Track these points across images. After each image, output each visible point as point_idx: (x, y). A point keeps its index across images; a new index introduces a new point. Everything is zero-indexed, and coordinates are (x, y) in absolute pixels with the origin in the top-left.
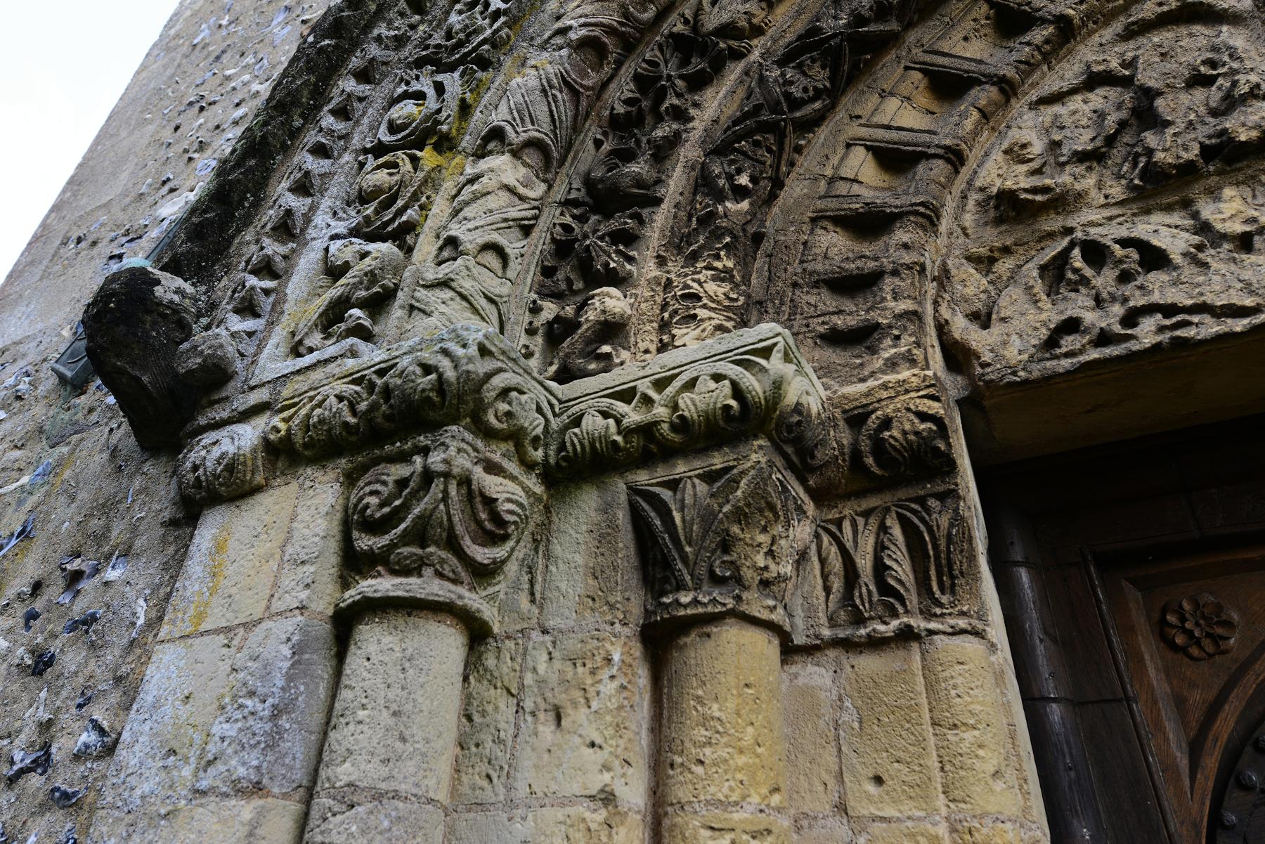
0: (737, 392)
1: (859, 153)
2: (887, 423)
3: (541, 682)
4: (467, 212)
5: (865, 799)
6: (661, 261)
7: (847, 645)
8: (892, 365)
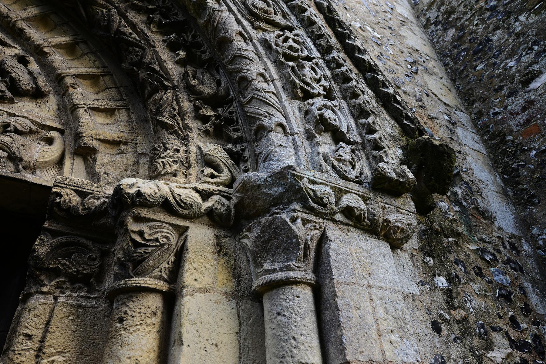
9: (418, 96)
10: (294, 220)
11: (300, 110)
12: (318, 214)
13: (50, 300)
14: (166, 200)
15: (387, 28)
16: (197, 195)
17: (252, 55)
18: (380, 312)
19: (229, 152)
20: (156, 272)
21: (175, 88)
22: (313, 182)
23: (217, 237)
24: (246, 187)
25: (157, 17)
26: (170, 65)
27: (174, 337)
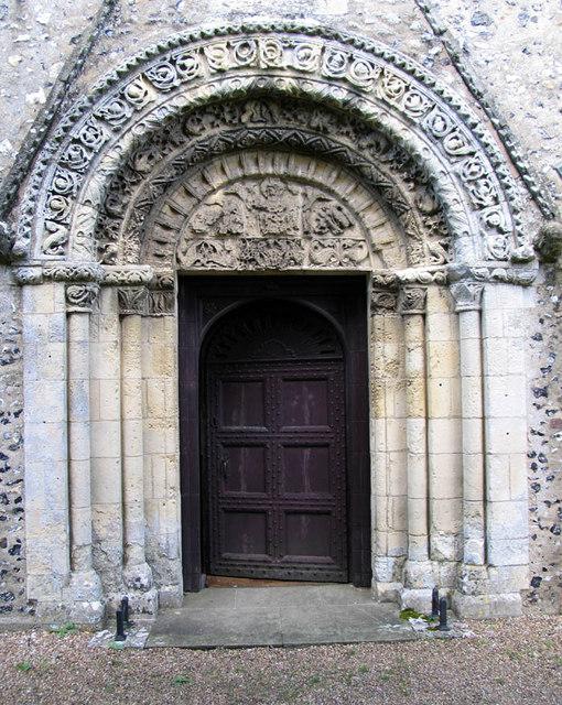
8: (166, 266)
17: (450, 187)
19: (442, 245)
24: (448, 269)
25: (395, 164)
26: (407, 194)
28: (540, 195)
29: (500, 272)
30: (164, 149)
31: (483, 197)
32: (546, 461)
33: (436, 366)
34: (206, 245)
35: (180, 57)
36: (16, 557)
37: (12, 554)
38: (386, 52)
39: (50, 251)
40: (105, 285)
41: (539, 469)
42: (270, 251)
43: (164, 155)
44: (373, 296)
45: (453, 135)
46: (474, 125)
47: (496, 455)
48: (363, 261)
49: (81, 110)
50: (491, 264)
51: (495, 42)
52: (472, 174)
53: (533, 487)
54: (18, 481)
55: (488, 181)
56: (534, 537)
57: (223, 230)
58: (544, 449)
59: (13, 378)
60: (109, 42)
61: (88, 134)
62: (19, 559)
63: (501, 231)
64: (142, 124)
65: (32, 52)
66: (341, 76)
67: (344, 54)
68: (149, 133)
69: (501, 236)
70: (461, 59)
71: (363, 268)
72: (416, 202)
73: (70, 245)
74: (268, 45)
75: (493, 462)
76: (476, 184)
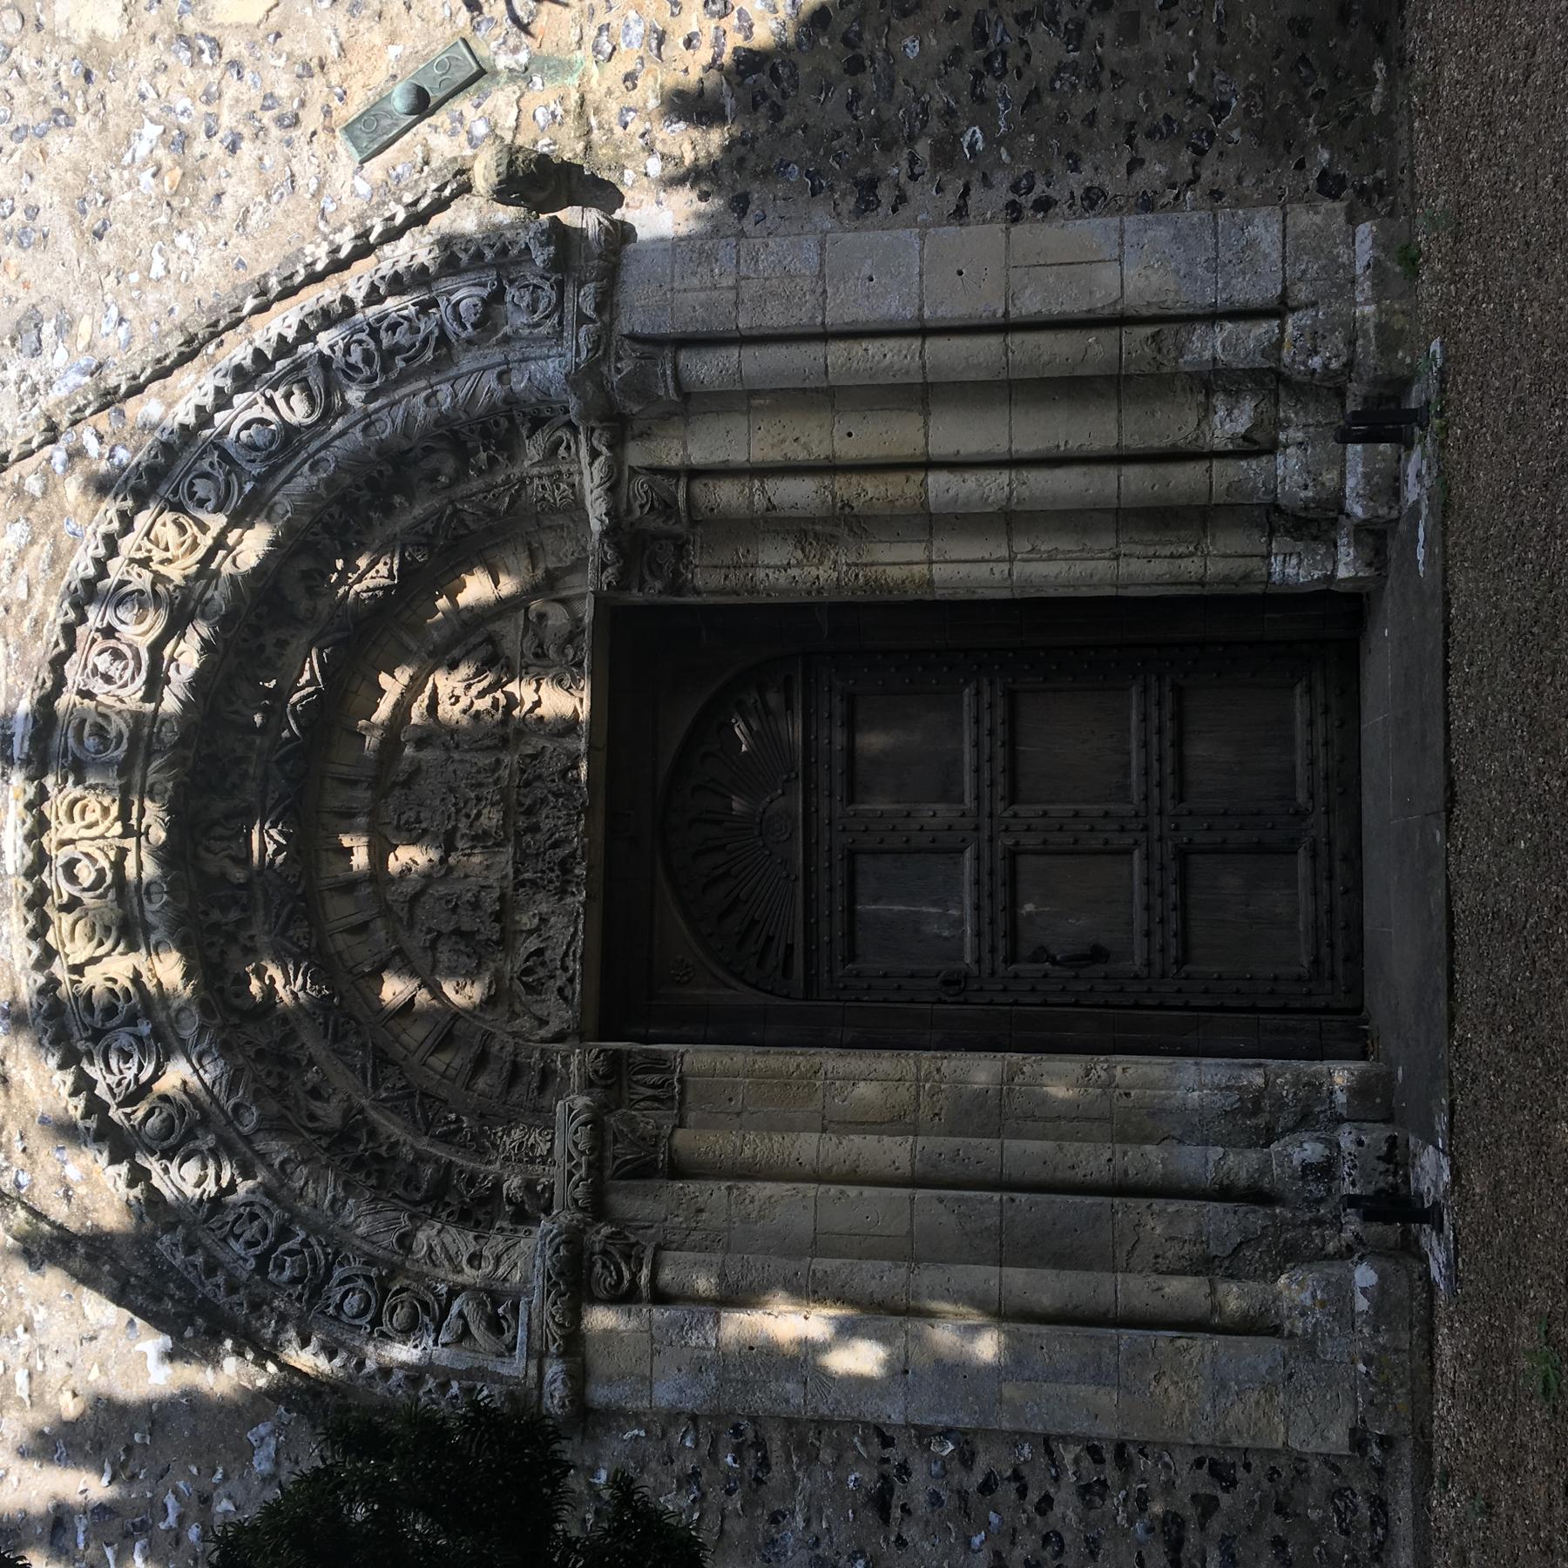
0: (584, 1124)
1: (432, 1060)
2: (596, 1072)
3: (686, 1219)
4: (452, 1252)
5: (736, 1105)
6: (489, 1162)
7: (682, 1103)
8: (566, 1065)
9: (298, 69)
10: (618, 371)
11: (467, 350)
12: (609, 344)
13: (698, 570)
14: (609, 489)
15: (93, 91)
16: (596, 464)
17: (399, 412)
18: (695, 281)
20: (673, 488)
21: (452, 502)
22: (578, 353)
23: (633, 438)
24: (584, 417)
26: (418, 511)
27: (722, 466)
28: (415, 203)
29: (585, 296)
30: (298, 1061)
31: (421, 335)
32: (1030, 175)
33: (805, 446)
34: (527, 972)
35: (88, 1020)
36: (1241, 1473)
37: (1234, 1483)
38: (91, 552)
39: (508, 1336)
40: (597, 1207)
41: (1050, 192)
42: (546, 825)
43: (311, 1062)
44: (652, 592)
45: (281, 403)
46: (258, 353)
47: (1010, 297)
48: (571, 612)
49: (190, 1250)
50: (570, 317)
51: (79, 303)
52: (368, 358)
53: (1092, 207)
54: (1049, 1452)
55: (385, 324)
56: (1216, 195)
57: (492, 931)
58: (1002, 181)
59: (801, 1445)
60: (42, 1181)
61: (247, 1236)
62: (1247, 1466)
63: (497, 296)
64: (237, 1107)
65: (57, 1365)
66: (145, 656)
67: (96, 648)
68: (257, 1096)
69: (508, 298)
70: (112, 382)
71: (587, 611)
72: (434, 492)
73: (497, 1286)
74: (71, 819)
75: (1030, 304)
76: (396, 350)
